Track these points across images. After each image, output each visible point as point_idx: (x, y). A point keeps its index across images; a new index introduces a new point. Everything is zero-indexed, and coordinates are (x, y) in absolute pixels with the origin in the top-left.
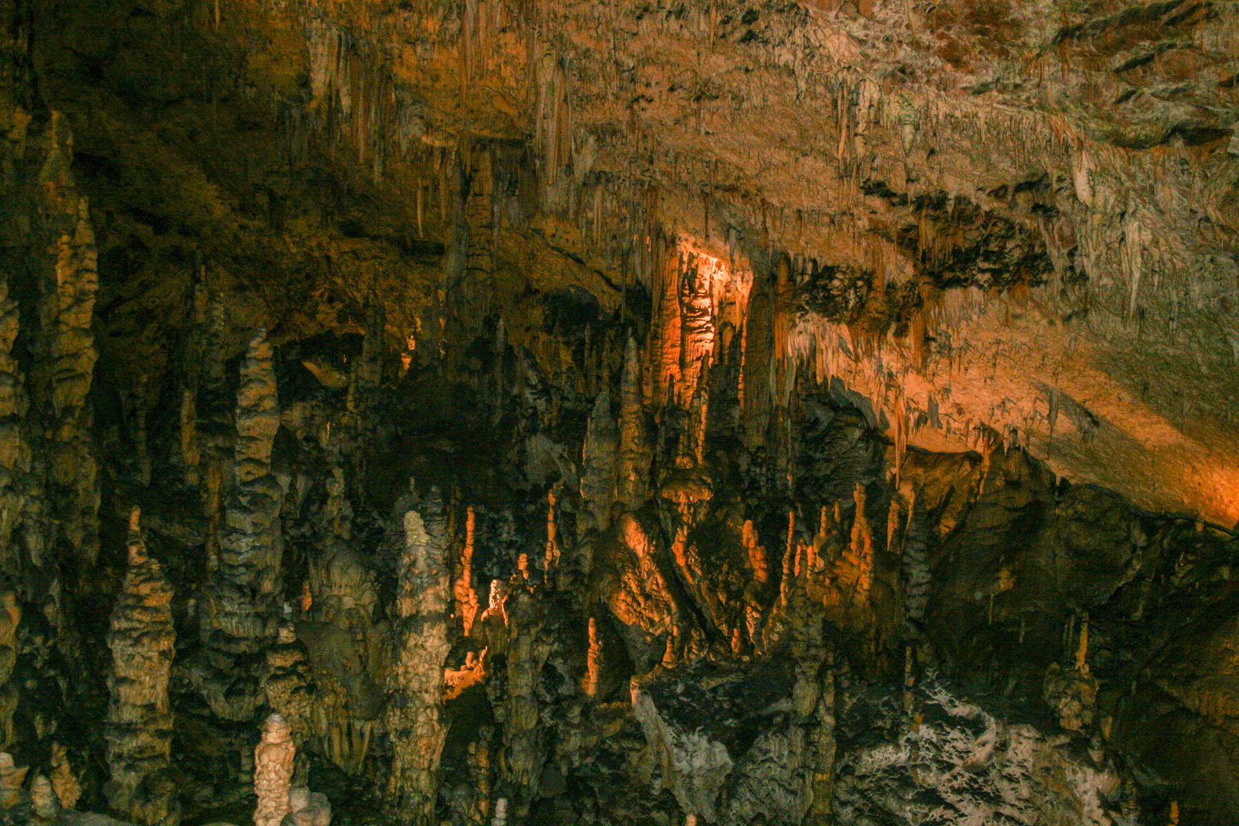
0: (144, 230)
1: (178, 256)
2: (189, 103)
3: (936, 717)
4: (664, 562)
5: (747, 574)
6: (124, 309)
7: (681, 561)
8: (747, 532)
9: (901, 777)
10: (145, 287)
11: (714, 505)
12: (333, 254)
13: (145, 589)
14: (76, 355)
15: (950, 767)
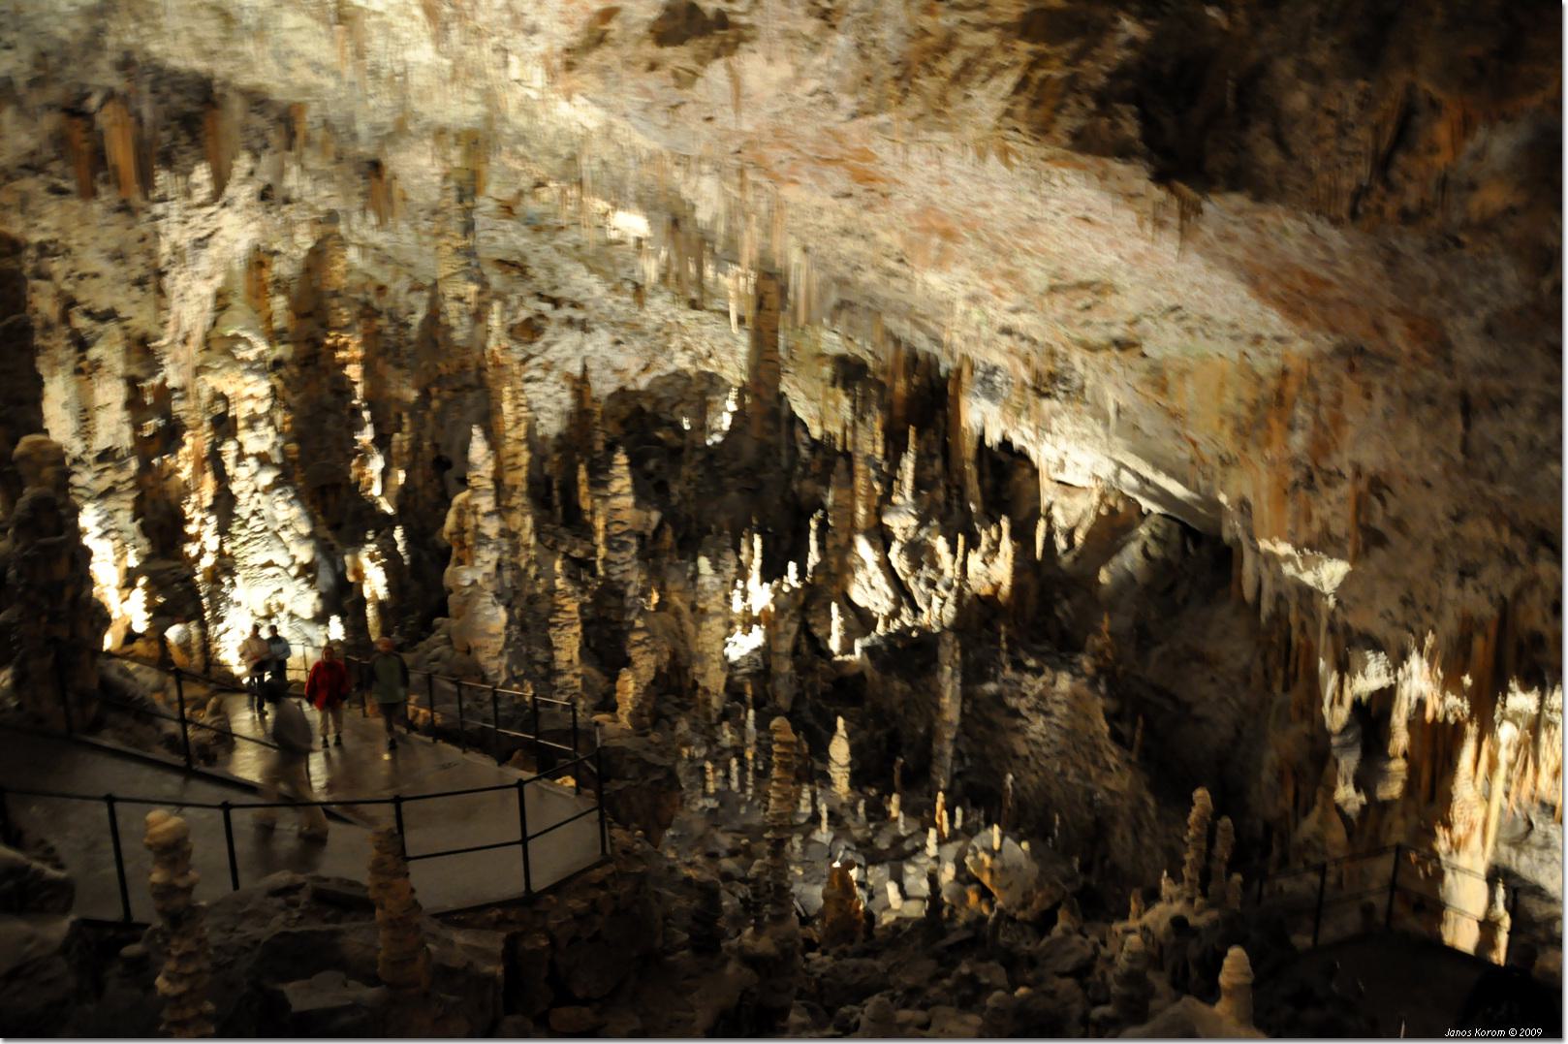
0: (546, 307)
1: (570, 322)
2: (574, 228)
3: (1019, 666)
4: (886, 566)
5: (941, 572)
6: (533, 362)
7: (895, 564)
8: (941, 544)
9: (998, 699)
10: (548, 345)
11: (919, 528)
12: (682, 321)
13: (564, 601)
14: (516, 455)
15: (1024, 695)
